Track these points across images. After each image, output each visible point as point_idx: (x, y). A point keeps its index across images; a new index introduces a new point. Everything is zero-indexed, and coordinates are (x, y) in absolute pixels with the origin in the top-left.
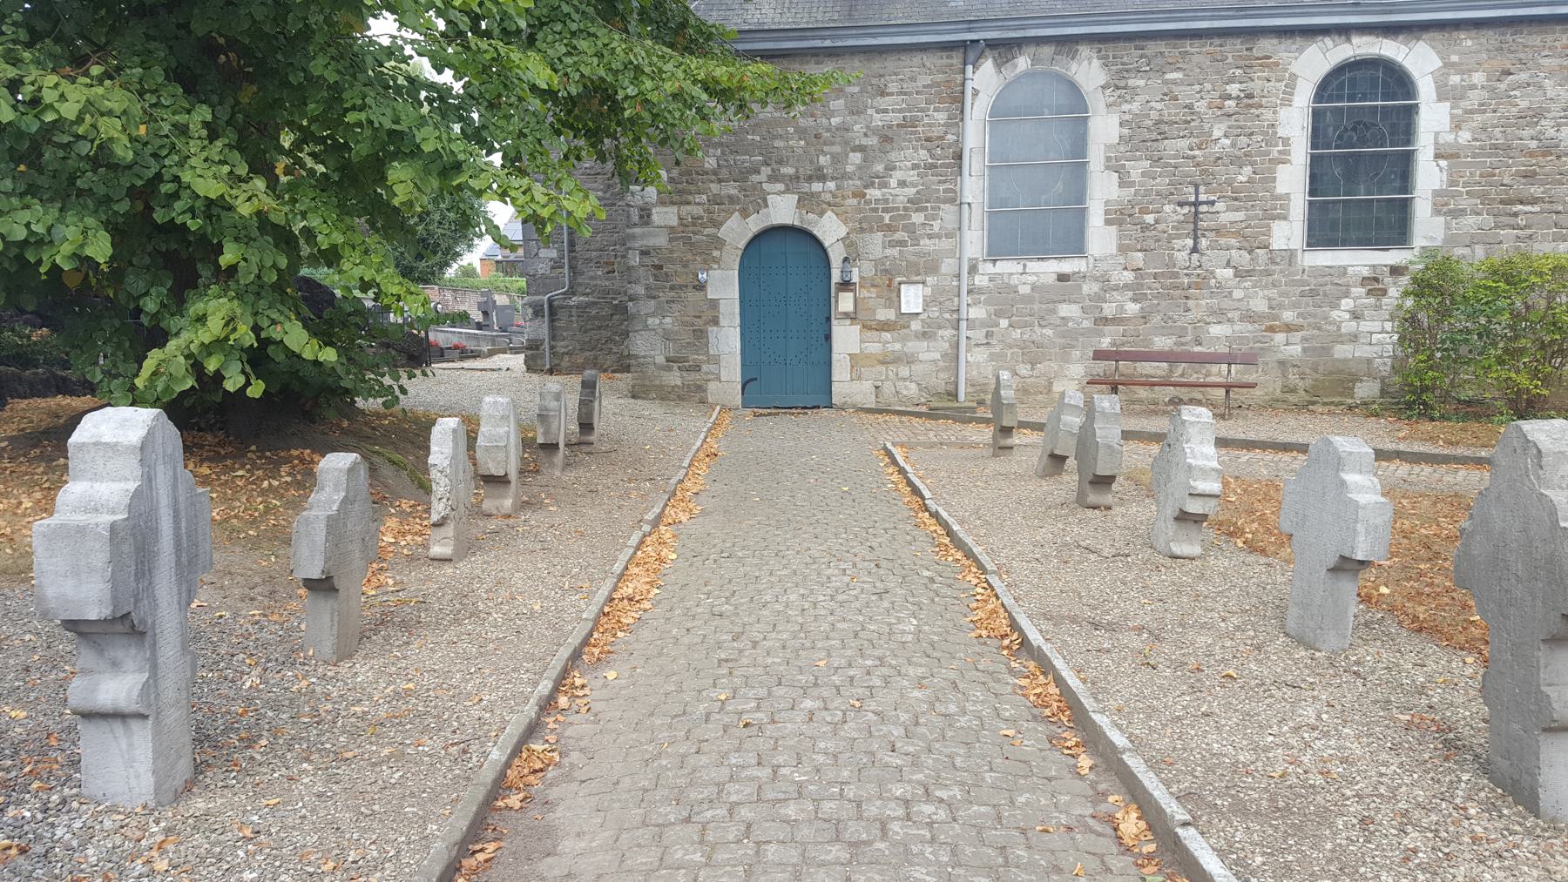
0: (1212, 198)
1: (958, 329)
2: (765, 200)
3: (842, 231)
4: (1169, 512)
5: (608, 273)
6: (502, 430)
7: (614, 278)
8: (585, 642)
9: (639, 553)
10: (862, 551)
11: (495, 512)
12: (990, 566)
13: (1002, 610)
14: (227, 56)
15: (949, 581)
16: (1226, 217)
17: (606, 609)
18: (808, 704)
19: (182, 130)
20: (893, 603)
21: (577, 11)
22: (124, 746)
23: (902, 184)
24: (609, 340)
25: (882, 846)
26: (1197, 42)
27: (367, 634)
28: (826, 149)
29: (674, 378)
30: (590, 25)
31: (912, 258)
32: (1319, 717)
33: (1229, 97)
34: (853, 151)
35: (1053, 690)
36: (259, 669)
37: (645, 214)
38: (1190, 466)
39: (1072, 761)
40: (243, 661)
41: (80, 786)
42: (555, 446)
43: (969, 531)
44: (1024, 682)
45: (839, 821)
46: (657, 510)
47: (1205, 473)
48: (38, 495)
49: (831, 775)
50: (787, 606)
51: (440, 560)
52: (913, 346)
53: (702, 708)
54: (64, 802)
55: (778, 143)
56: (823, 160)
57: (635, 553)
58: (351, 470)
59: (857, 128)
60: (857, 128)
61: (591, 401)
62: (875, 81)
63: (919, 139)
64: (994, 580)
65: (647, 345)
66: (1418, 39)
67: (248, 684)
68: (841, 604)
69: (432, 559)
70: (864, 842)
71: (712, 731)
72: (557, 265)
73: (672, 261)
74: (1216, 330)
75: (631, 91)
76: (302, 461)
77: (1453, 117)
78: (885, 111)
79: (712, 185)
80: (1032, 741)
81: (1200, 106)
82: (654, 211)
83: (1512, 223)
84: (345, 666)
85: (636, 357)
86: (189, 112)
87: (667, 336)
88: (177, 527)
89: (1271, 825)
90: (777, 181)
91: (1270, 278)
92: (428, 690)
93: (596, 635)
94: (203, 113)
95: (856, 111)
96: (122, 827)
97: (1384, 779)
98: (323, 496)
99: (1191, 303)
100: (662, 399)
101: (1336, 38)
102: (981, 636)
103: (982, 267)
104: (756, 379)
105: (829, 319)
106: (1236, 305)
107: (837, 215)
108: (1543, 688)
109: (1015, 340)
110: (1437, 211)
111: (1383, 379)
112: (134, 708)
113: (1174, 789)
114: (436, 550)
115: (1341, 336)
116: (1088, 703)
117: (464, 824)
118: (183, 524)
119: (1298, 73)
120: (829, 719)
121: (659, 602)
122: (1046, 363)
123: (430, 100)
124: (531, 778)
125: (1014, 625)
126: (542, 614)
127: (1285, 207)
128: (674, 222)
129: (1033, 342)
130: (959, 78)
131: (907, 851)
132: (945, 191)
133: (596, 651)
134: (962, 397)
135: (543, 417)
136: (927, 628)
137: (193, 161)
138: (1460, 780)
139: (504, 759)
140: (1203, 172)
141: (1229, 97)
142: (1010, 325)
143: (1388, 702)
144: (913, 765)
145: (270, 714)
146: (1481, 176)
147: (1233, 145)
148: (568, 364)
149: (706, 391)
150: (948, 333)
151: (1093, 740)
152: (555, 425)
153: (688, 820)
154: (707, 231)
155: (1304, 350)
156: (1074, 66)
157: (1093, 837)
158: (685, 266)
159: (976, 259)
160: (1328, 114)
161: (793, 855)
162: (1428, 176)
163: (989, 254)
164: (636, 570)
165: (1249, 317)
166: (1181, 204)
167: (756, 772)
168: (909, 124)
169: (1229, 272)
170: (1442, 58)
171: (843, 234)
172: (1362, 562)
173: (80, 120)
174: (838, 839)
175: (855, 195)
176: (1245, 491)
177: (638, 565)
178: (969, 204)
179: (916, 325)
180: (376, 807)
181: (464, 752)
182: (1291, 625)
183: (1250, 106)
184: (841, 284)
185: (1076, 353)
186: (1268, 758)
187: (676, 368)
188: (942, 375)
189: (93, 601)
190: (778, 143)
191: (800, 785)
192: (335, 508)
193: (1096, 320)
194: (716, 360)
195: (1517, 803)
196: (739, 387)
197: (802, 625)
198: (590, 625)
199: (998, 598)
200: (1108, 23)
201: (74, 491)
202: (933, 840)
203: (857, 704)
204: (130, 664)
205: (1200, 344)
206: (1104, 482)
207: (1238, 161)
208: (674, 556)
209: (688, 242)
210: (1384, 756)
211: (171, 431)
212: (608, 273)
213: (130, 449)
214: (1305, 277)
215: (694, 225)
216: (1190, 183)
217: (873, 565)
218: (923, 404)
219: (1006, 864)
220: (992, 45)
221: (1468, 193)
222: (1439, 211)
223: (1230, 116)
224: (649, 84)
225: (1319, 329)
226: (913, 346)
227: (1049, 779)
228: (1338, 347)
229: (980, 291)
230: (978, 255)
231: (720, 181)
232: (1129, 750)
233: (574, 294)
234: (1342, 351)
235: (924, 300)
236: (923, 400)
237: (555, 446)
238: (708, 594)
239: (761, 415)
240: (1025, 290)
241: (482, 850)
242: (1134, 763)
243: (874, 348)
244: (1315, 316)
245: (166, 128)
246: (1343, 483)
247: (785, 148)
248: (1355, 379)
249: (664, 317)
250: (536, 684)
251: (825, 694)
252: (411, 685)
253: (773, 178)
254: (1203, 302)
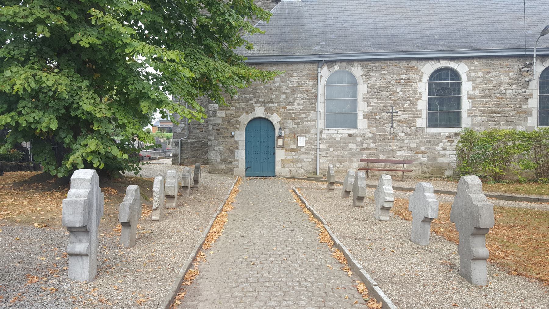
0: (397, 111)
1: (316, 151)
2: (254, 109)
3: (279, 119)
4: (379, 207)
5: (201, 132)
6: (173, 181)
7: (203, 134)
8: (203, 244)
9: (216, 219)
10: (287, 219)
11: (170, 207)
12: (325, 223)
13: (328, 235)
14: (89, 65)
15: (313, 227)
16: (402, 117)
17: (208, 235)
18: (271, 259)
19: (80, 88)
20: (296, 233)
21: (198, 52)
22: (81, 264)
23: (298, 104)
24: (201, 154)
25: (293, 292)
26: (391, 62)
27: (137, 241)
28: (274, 93)
29: (223, 167)
30: (202, 56)
31: (302, 128)
32: (417, 261)
33: (402, 79)
34: (283, 94)
35: (342, 255)
36: (108, 249)
37: (215, 113)
38: (385, 193)
39: (347, 273)
40: (102, 247)
41: (68, 276)
42: (187, 187)
43: (319, 213)
44: (334, 254)
45: (281, 286)
46: (221, 207)
47: (389, 195)
48: (28, 200)
49: (278, 276)
50: (264, 234)
51: (155, 221)
52: (302, 157)
53: (240, 260)
54: (64, 279)
55: (258, 91)
56: (273, 97)
57: (215, 220)
58: (136, 190)
59: (284, 87)
60: (284, 87)
61: (198, 173)
62: (289, 72)
63: (304, 91)
64: (326, 227)
65: (214, 156)
66: (461, 62)
67: (105, 253)
68: (280, 233)
69: (153, 221)
70: (288, 291)
71: (244, 266)
72: (184, 129)
73: (223, 128)
74: (399, 153)
75: (215, 76)
76: (108, 191)
77: (473, 86)
78: (293, 82)
79: (237, 104)
80: (336, 268)
81: (393, 82)
82: (217, 112)
83: (492, 120)
84: (132, 249)
85: (211, 159)
86: (82, 82)
87: (221, 153)
88: (97, 203)
89: (399, 286)
90: (258, 103)
91: (416, 137)
92: (159, 255)
93: (206, 242)
94: (86, 82)
95: (284, 81)
96: (81, 286)
97: (432, 276)
98: (128, 198)
99: (391, 144)
100: (219, 174)
101: (435, 61)
102: (322, 242)
103: (324, 131)
104: (250, 167)
105: (274, 148)
106: (406, 145)
107: (277, 114)
108: (471, 248)
109: (335, 155)
110: (469, 116)
111: (454, 169)
112: (85, 253)
113: (374, 278)
114: (154, 218)
115: (439, 155)
116: (352, 258)
117: (176, 287)
118: (98, 202)
119: (424, 72)
120: (277, 263)
121: (224, 233)
122: (345, 163)
123: (153, 79)
124: (192, 278)
125: (332, 239)
126: (189, 236)
127: (421, 114)
128: (224, 116)
129: (341, 156)
130: (316, 72)
131: (300, 293)
132: (312, 107)
133: (206, 246)
134: (318, 173)
135: (184, 178)
136: (306, 240)
137: (83, 98)
138: (452, 276)
139: (184, 272)
140: (394, 103)
141: (402, 79)
142: (334, 150)
143: (438, 258)
144: (301, 273)
145: (114, 261)
146: (482, 105)
147: (404, 94)
148: (187, 162)
149: (233, 171)
150: (313, 152)
151: (353, 267)
152: (187, 181)
153: (238, 287)
154: (235, 119)
155: (428, 159)
156: (353, 69)
157: (351, 290)
158: (228, 130)
159: (322, 129)
160: (434, 85)
161: (269, 294)
162: (466, 105)
163: (326, 128)
164: (216, 224)
165: (410, 149)
166: (387, 113)
167: (257, 275)
168: (300, 86)
169: (403, 134)
170: (469, 68)
171: (279, 120)
172: (431, 219)
173: (53, 86)
174: (280, 291)
175: (283, 108)
176: (405, 203)
177: (216, 223)
178: (320, 111)
179: (303, 150)
180: (150, 283)
181: (173, 270)
182: (412, 238)
183: (409, 82)
184: (278, 136)
185: (355, 160)
186: (401, 271)
187: (224, 163)
188: (311, 166)
189: (77, 221)
190: (258, 91)
191: (270, 278)
192: (131, 201)
193: (361, 149)
194: (237, 161)
195: (466, 281)
196: (245, 170)
197: (268, 239)
198: (204, 239)
199: (327, 232)
200: (363, 56)
201: (72, 191)
202: (307, 291)
203: (286, 259)
204: (84, 240)
205: (394, 157)
206: (361, 199)
207: (405, 99)
208: (227, 221)
209: (228, 122)
210: (433, 270)
211: (97, 176)
212: (201, 132)
213: (88, 180)
214: (428, 136)
215: (231, 117)
216: (390, 106)
217: (290, 223)
218: (305, 176)
219: (327, 296)
220: (327, 62)
221: (478, 110)
222: (470, 116)
223: (402, 85)
224: (220, 75)
225: (433, 153)
226: (302, 157)
227: (340, 277)
228: (439, 159)
229: (324, 139)
230: (323, 128)
231: (239, 103)
232: (362, 269)
233: (189, 139)
234: (440, 160)
235: (306, 142)
236: (305, 174)
237: (187, 187)
238: (239, 231)
239: (252, 179)
240: (338, 139)
241: (181, 294)
242: (363, 272)
243: (290, 157)
244: (431, 149)
245: (75, 88)
246: (425, 196)
247: (261, 93)
248: (445, 169)
249: (220, 146)
250: (190, 254)
251: (276, 256)
252: (153, 254)
253: (257, 102)
254: (395, 144)
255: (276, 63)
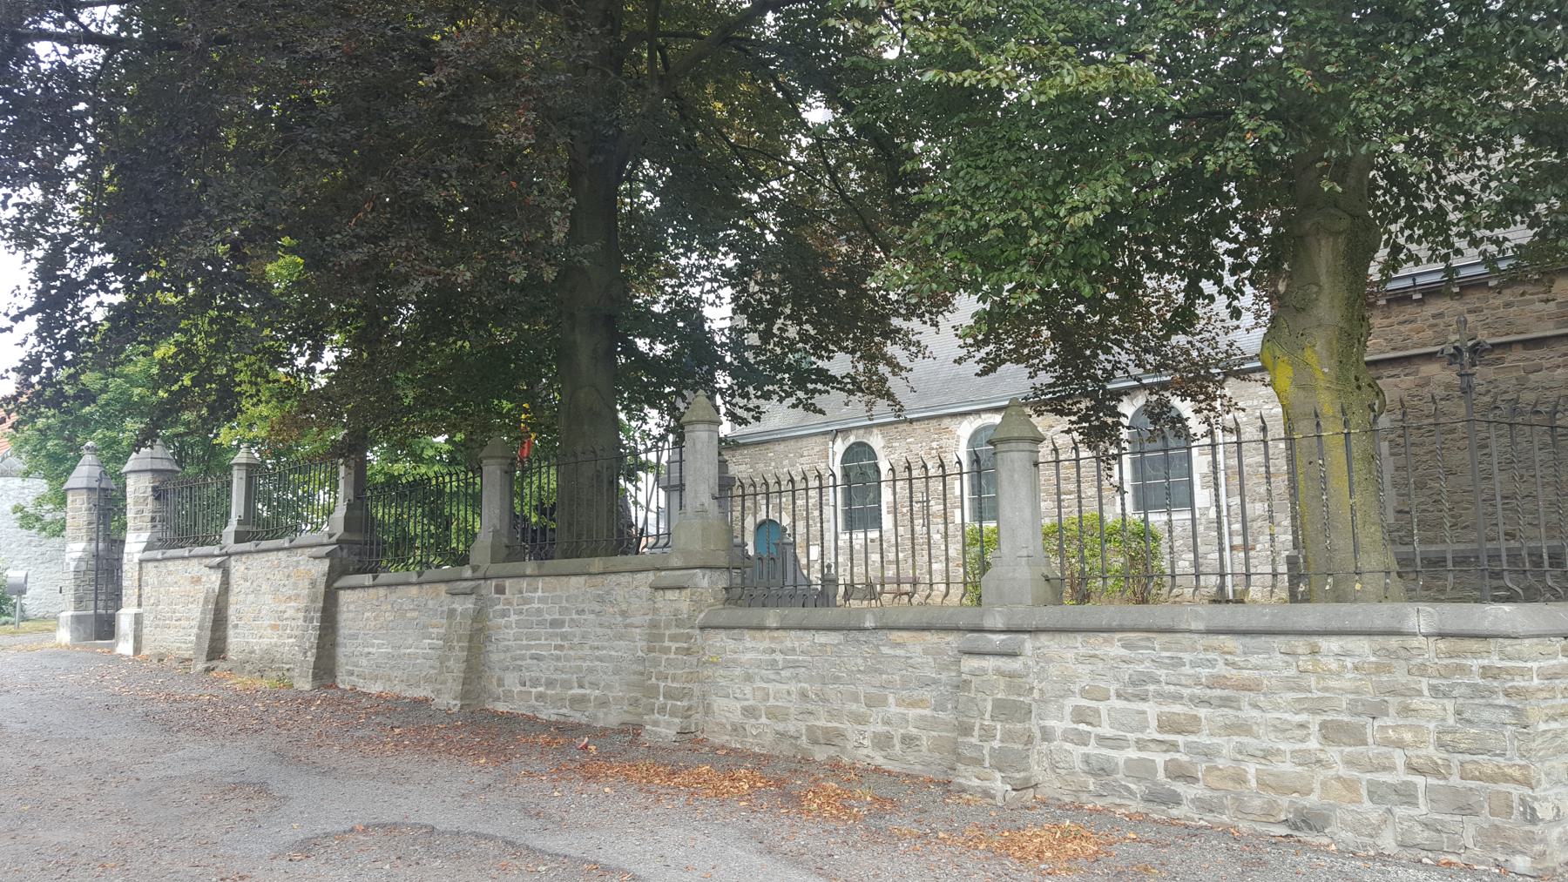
255: (777, 440)
